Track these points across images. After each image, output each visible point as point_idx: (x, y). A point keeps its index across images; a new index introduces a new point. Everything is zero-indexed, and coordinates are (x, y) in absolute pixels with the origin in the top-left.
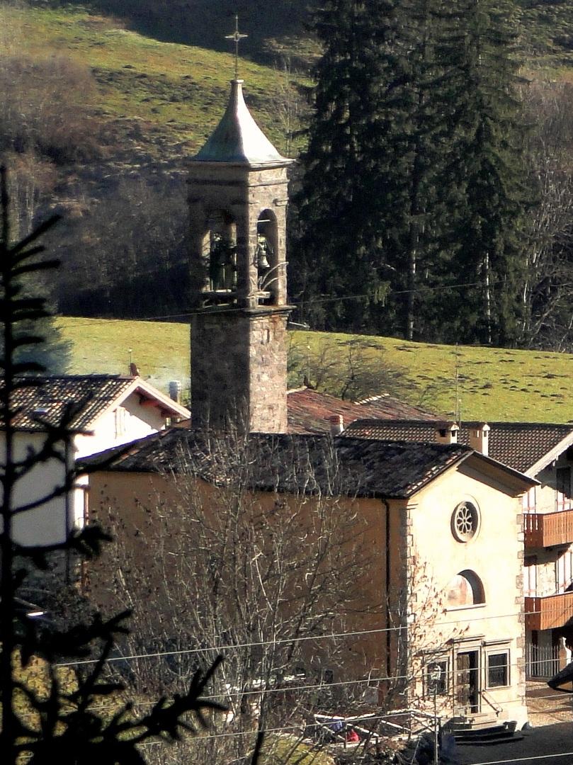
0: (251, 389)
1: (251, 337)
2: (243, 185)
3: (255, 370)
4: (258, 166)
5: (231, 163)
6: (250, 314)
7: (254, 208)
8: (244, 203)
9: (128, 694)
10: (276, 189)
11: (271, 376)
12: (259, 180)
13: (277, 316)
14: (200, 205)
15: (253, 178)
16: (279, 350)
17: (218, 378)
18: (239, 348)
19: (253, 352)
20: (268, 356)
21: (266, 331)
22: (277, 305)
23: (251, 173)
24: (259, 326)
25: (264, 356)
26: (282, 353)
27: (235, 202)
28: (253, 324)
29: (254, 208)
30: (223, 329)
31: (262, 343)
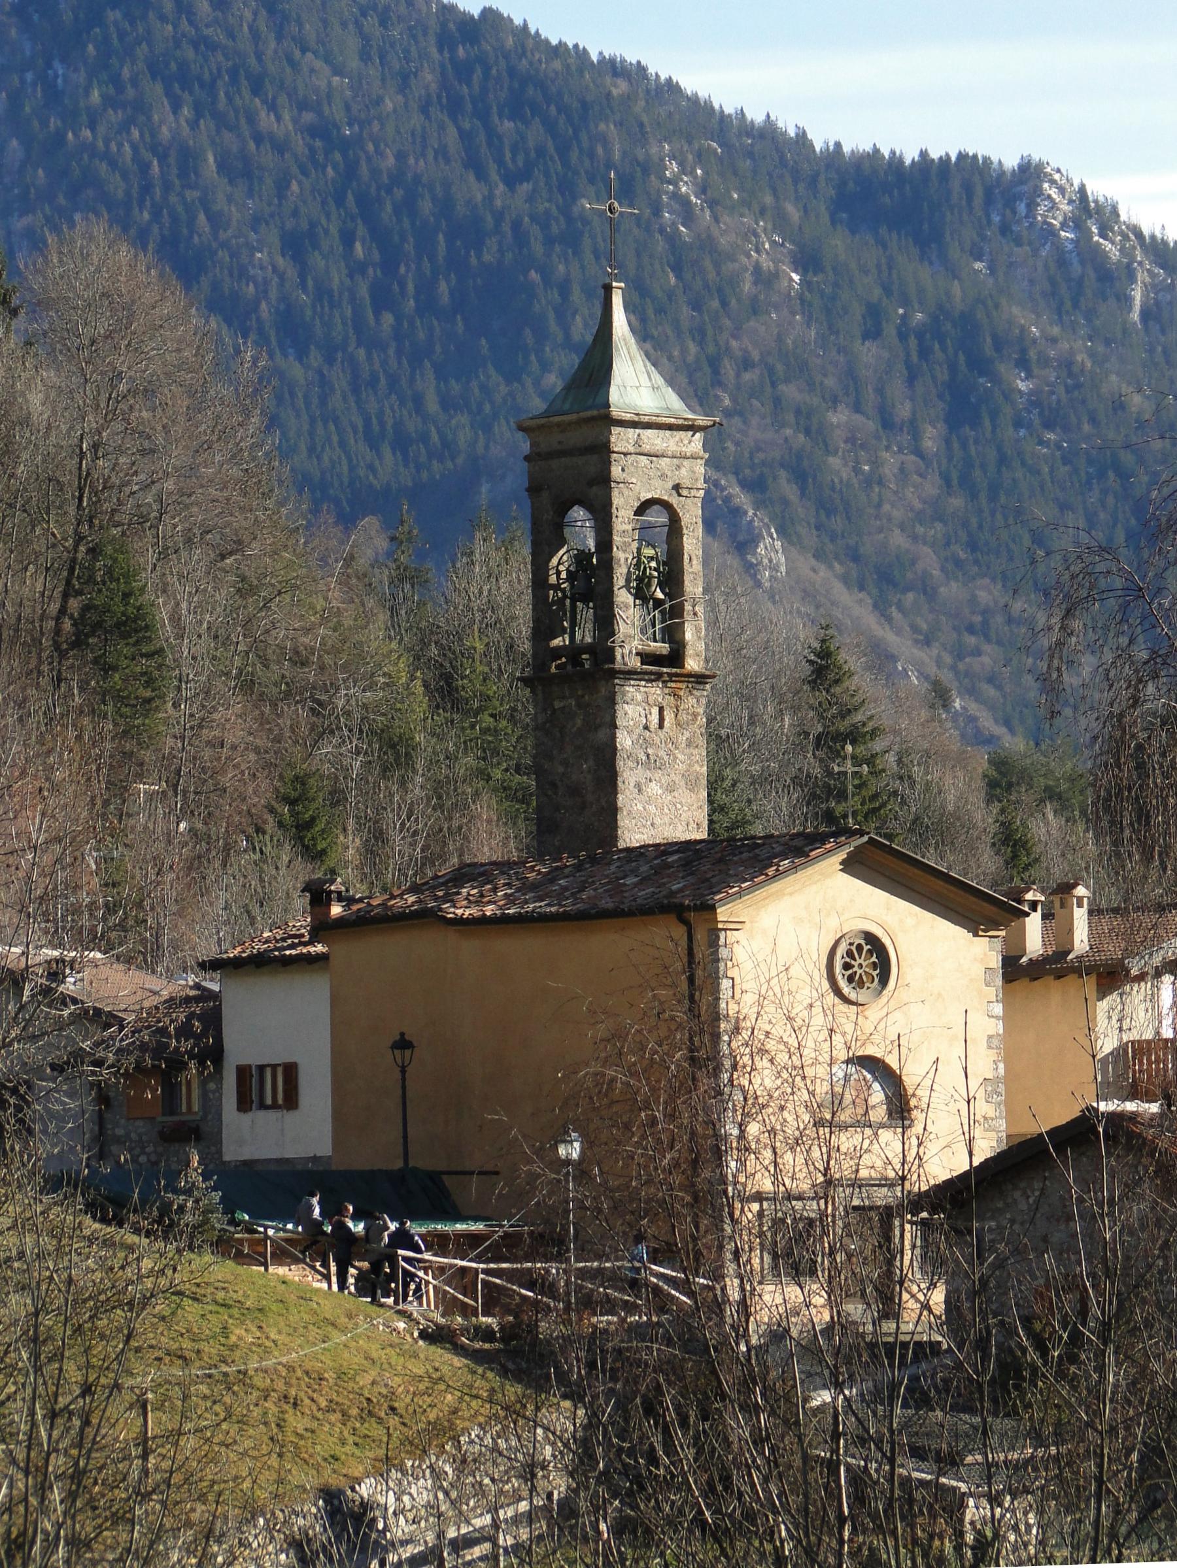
0: (619, 804)
1: (619, 714)
2: (603, 451)
3: (629, 775)
4: (628, 417)
5: (582, 415)
6: (614, 673)
7: (626, 492)
8: (604, 481)
9: (1031, 1521)
10: (678, 467)
11: (670, 789)
12: (637, 443)
13: (683, 686)
14: (545, 495)
15: (621, 439)
16: (688, 745)
17: (575, 791)
18: (602, 735)
19: (624, 740)
20: (662, 753)
21: (655, 710)
22: (683, 667)
23: (615, 430)
24: (639, 697)
25: (650, 751)
26: (695, 752)
27: (591, 483)
28: (624, 694)
29: (626, 492)
30: (579, 705)
31: (646, 728)
